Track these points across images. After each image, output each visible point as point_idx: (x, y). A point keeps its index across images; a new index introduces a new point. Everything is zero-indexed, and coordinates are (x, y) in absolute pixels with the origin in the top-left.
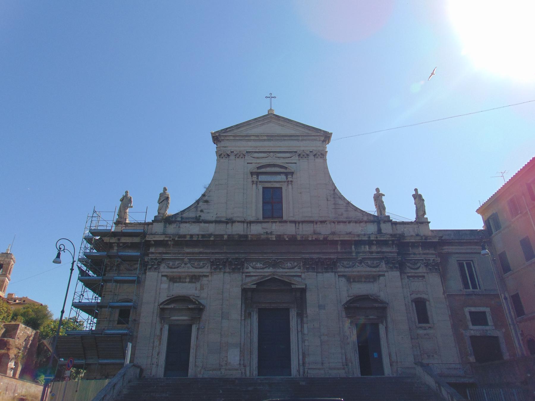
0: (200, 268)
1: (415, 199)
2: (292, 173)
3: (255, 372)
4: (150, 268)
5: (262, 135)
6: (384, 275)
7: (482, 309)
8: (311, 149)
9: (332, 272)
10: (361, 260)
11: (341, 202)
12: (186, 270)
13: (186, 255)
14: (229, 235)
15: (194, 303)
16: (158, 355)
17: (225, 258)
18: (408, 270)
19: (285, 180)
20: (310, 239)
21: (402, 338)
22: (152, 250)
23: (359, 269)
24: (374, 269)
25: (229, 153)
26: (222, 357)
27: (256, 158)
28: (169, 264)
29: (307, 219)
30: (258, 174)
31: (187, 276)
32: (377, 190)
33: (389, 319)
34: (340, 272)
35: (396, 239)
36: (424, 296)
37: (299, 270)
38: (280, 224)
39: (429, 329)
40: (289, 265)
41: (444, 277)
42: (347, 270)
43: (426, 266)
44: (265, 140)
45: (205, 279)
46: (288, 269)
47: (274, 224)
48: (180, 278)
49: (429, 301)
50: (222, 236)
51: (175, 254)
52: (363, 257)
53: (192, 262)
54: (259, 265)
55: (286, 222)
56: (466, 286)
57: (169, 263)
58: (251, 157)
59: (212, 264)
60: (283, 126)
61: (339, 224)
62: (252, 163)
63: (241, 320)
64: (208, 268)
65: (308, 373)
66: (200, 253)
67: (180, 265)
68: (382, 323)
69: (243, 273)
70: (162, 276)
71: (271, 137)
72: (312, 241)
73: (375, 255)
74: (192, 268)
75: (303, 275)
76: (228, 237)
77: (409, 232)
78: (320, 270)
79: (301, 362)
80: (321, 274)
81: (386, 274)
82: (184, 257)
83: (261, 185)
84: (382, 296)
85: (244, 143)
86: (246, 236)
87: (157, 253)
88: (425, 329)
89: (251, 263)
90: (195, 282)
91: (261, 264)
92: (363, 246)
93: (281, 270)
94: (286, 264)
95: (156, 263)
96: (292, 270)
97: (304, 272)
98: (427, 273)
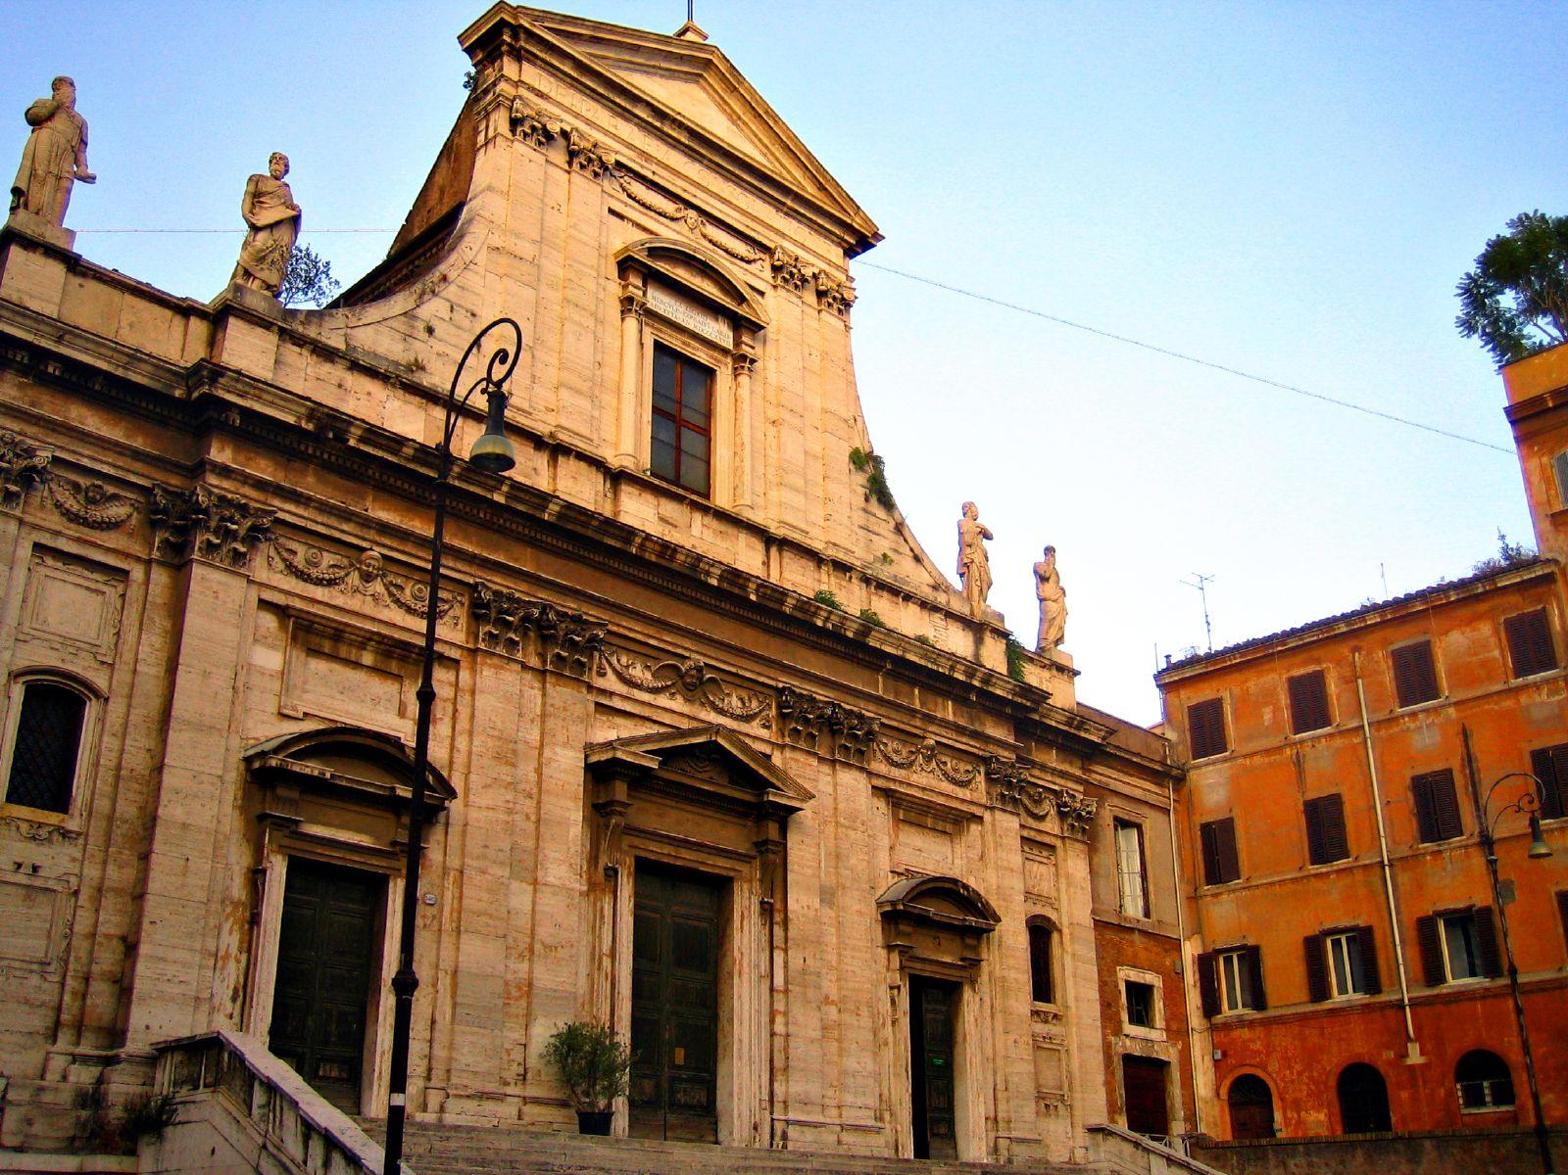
4: (210, 548)
5: (679, 117)
6: (980, 820)
9: (862, 769)
10: (932, 749)
12: (369, 609)
13: (372, 535)
14: (570, 506)
16: (234, 999)
17: (534, 604)
19: (731, 348)
20: (820, 623)
21: (1015, 1042)
22: (220, 453)
26: (506, 1046)
27: (638, 202)
28: (294, 553)
30: (652, 277)
31: (370, 639)
32: (969, 510)
33: (984, 978)
34: (878, 776)
35: (1029, 704)
36: (1053, 916)
37: (764, 733)
38: (715, 524)
39: (1054, 1021)
40: (735, 702)
42: (896, 773)
43: (1062, 816)
44: (675, 144)
46: (734, 717)
47: (698, 517)
49: (1060, 931)
50: (544, 498)
51: (324, 508)
52: (938, 739)
53: (391, 578)
54: (638, 672)
57: (294, 546)
58: (624, 190)
61: (880, 592)
62: (621, 217)
63: (581, 894)
64: (456, 624)
65: (785, 1136)
67: (342, 573)
68: (973, 982)
69: (590, 688)
70: (264, 604)
71: (700, 145)
72: (822, 631)
74: (393, 606)
76: (560, 516)
80: (826, 769)
81: (987, 816)
82: (364, 539)
83: (650, 330)
87: (246, 479)
88: (1046, 1022)
89: (612, 654)
90: (398, 678)
91: (648, 667)
92: (940, 700)
93: (713, 717)
94: (728, 695)
95: (242, 533)
97: (782, 747)
98: (1063, 838)
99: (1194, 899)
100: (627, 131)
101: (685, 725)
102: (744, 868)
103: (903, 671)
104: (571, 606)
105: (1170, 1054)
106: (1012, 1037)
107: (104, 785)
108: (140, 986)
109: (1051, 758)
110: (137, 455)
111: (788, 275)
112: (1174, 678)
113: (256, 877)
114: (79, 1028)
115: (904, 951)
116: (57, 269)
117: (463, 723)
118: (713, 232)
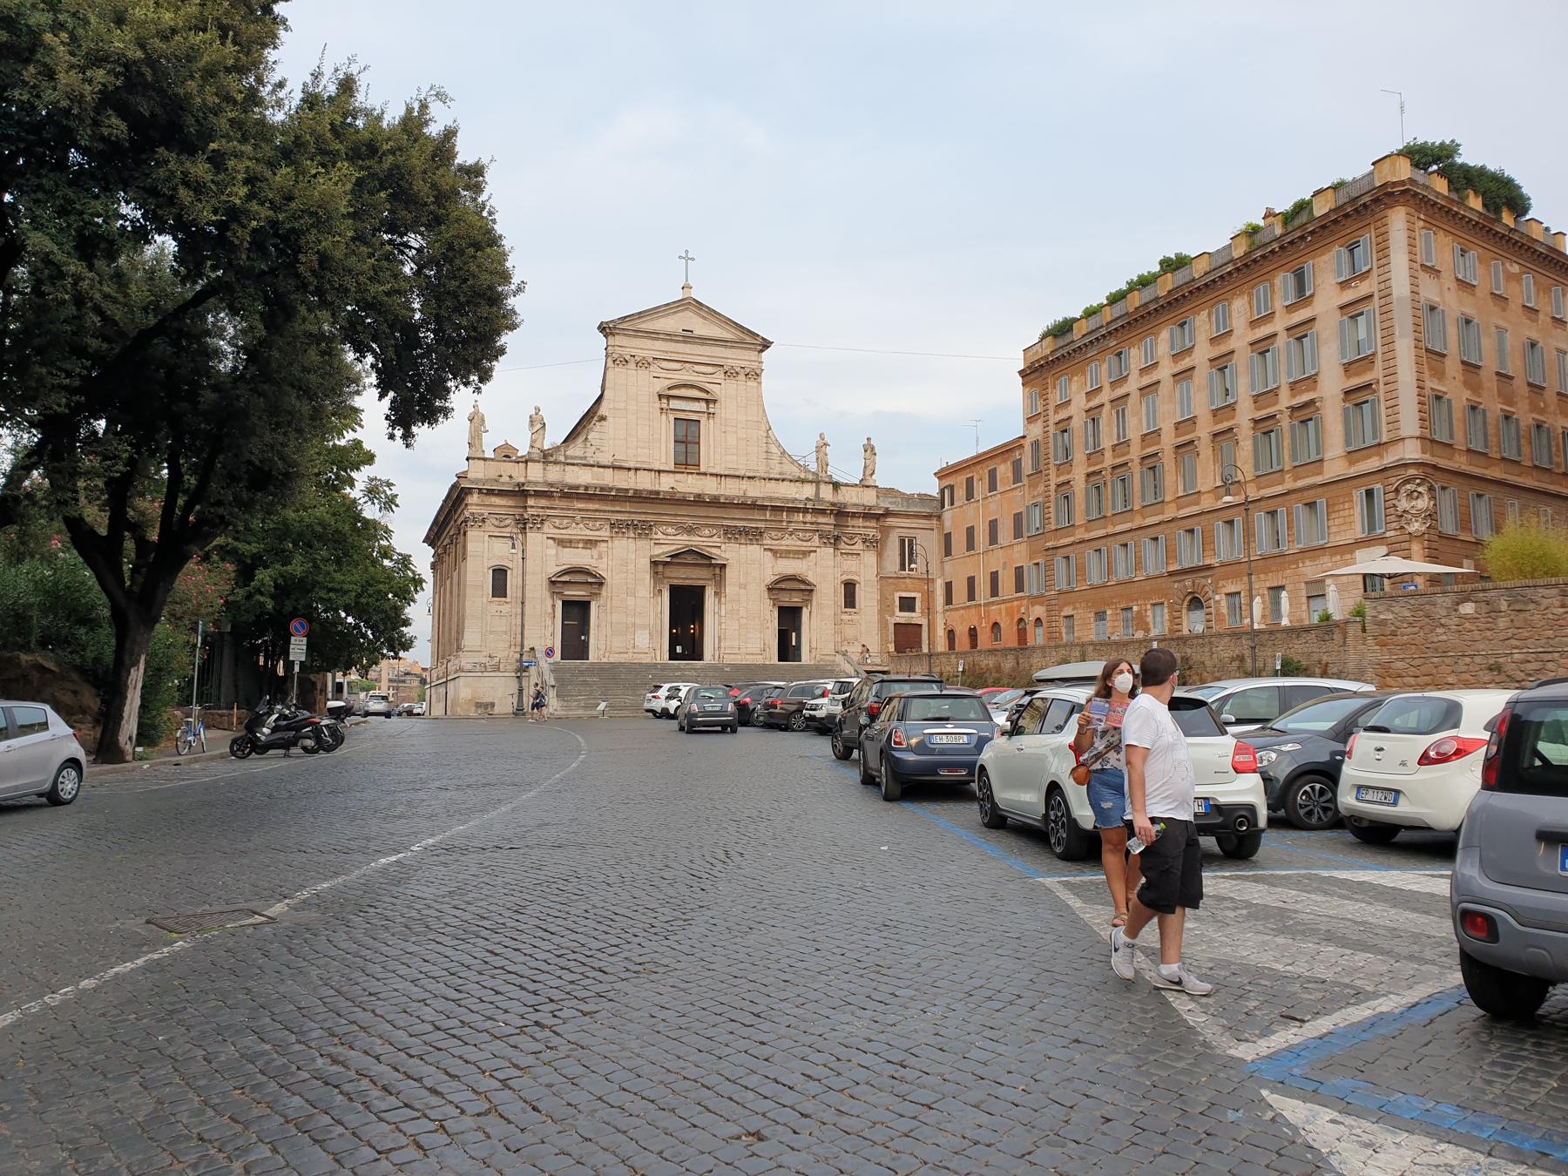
0: (598, 530)
1: (866, 451)
2: (715, 401)
3: (667, 656)
7: (912, 595)
8: (743, 364)
11: (774, 449)
15: (595, 576)
18: (842, 545)
22: (531, 502)
23: (789, 542)
24: (805, 544)
25: (628, 358)
29: (732, 473)
30: (669, 397)
33: (814, 603)
38: (698, 477)
40: (707, 531)
41: (880, 555)
42: (774, 542)
44: (678, 341)
45: (603, 545)
47: (690, 476)
48: (571, 541)
50: (627, 490)
51: (563, 509)
54: (670, 530)
55: (705, 474)
56: (903, 567)
59: (612, 526)
60: (705, 318)
66: (596, 511)
71: (688, 337)
73: (808, 526)
75: (723, 546)
77: (849, 497)
78: (743, 541)
79: (716, 646)
81: (818, 550)
84: (810, 579)
85: (648, 343)
86: (658, 493)
87: (538, 507)
96: (711, 539)
99: (942, 562)
100: (659, 345)
101: (687, 543)
102: (710, 582)
103: (776, 509)
104: (643, 517)
105: (924, 622)
106: (823, 623)
107: (514, 590)
108: (526, 636)
109: (860, 522)
110: (510, 507)
111: (730, 373)
112: (942, 475)
113: (554, 606)
114: (515, 645)
115: (774, 600)
116: (482, 462)
117: (610, 557)
118: (698, 368)
